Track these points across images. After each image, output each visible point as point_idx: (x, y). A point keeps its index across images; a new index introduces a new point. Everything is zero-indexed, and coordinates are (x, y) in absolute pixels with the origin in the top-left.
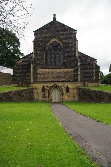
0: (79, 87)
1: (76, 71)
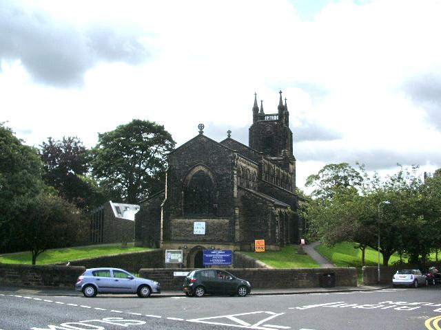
1: (232, 224)
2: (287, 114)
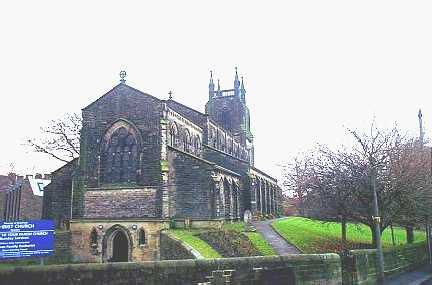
0: (164, 232)
1: (159, 194)
2: (243, 91)
